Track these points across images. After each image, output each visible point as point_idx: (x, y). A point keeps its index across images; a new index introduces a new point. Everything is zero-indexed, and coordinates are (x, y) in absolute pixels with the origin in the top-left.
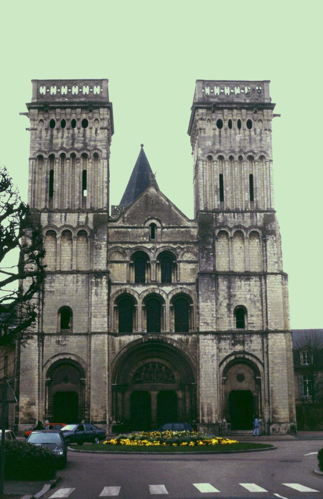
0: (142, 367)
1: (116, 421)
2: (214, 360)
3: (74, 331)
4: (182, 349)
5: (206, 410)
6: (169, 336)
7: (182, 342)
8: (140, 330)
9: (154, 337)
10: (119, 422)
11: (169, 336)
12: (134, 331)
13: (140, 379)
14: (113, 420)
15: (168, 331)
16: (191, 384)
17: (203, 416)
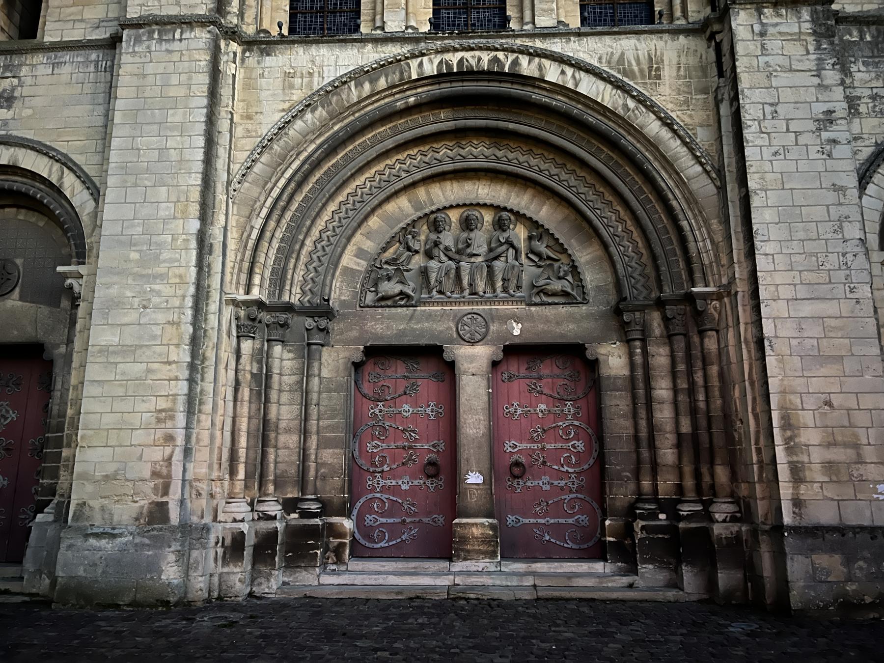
0: (410, 229)
1: (251, 504)
2: (834, 142)
3: (49, 38)
4: (625, 106)
5: (810, 436)
6: (556, 46)
7: (627, 73)
8: (394, 25)
9: (467, 55)
10: (274, 509)
11: (556, 46)
12: (364, 29)
13: (398, 288)
14: (231, 497)
15: (543, 21)
16: (690, 298)
17: (797, 474)
